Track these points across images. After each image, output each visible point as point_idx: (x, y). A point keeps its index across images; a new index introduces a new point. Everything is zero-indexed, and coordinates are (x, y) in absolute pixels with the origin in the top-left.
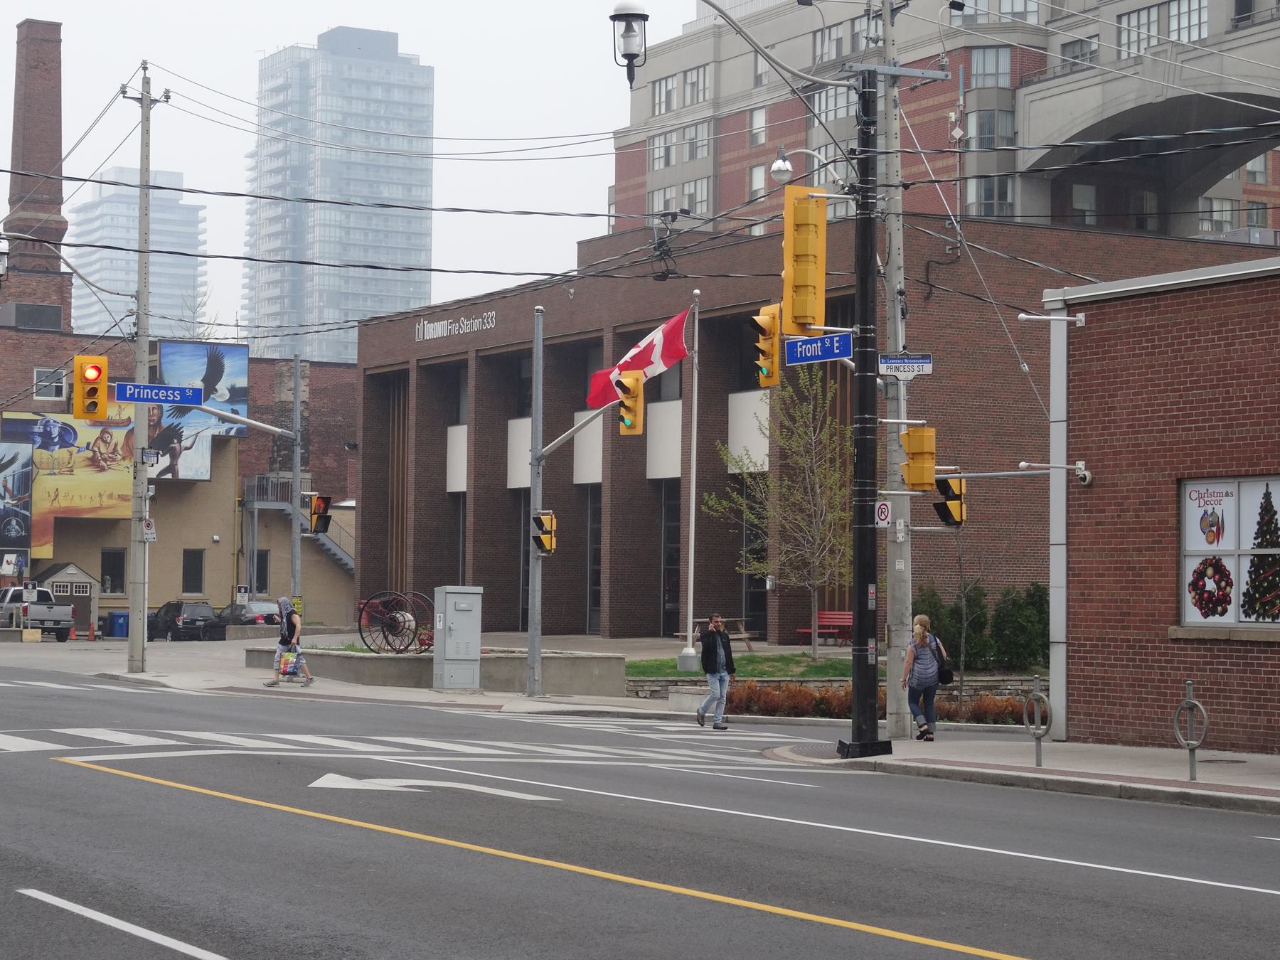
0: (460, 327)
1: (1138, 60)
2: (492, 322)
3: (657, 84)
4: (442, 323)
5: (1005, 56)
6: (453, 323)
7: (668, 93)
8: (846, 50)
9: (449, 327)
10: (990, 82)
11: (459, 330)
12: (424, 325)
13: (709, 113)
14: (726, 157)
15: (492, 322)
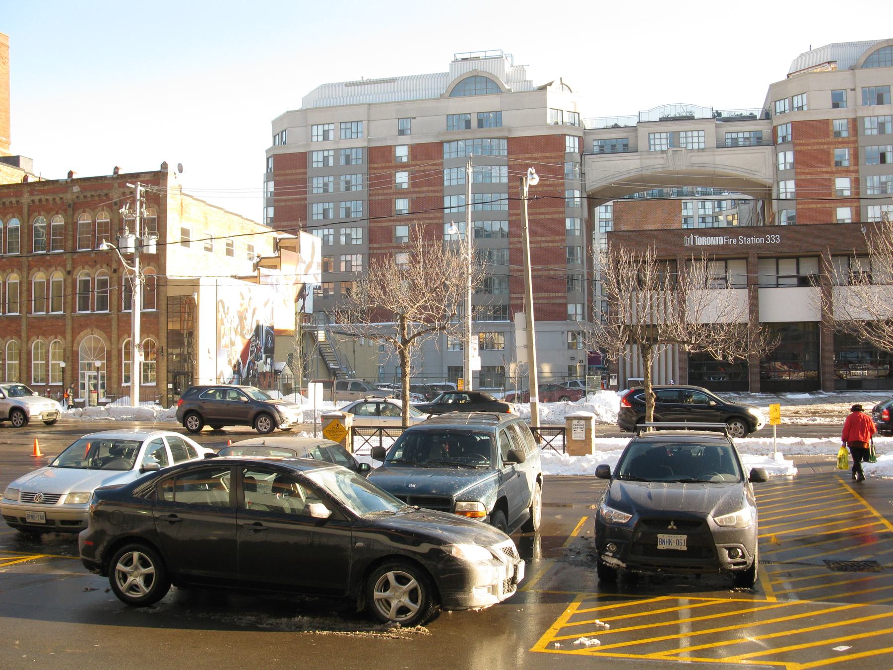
0: (738, 240)
1: (662, 152)
2: (776, 239)
3: (315, 128)
4: (717, 238)
5: (576, 139)
6: (730, 238)
7: (326, 134)
8: (474, 124)
9: (725, 240)
10: (572, 150)
11: (737, 242)
12: (694, 238)
13: (365, 144)
14: (376, 165)
15: (776, 239)
